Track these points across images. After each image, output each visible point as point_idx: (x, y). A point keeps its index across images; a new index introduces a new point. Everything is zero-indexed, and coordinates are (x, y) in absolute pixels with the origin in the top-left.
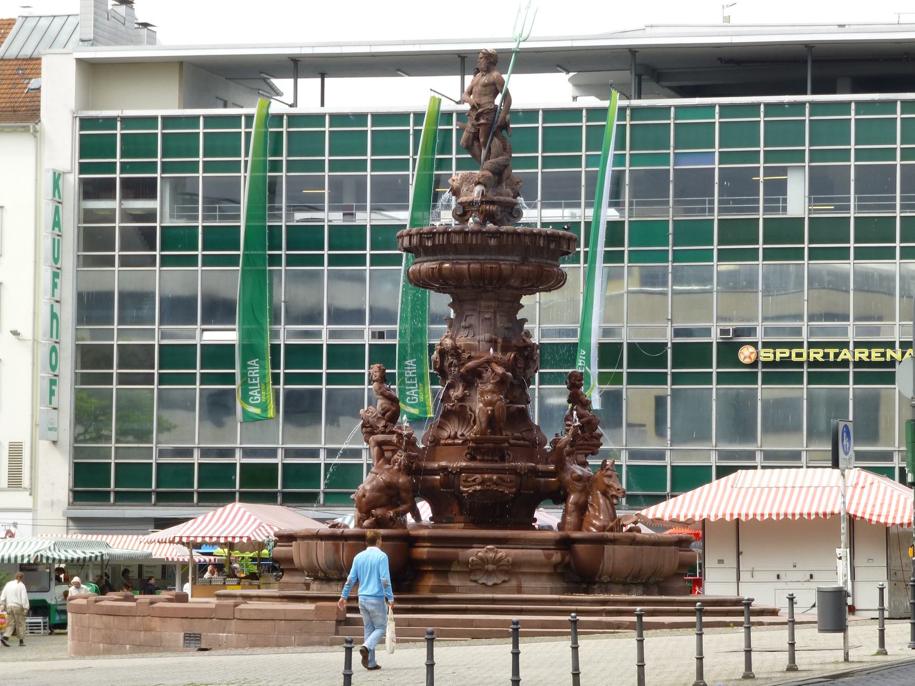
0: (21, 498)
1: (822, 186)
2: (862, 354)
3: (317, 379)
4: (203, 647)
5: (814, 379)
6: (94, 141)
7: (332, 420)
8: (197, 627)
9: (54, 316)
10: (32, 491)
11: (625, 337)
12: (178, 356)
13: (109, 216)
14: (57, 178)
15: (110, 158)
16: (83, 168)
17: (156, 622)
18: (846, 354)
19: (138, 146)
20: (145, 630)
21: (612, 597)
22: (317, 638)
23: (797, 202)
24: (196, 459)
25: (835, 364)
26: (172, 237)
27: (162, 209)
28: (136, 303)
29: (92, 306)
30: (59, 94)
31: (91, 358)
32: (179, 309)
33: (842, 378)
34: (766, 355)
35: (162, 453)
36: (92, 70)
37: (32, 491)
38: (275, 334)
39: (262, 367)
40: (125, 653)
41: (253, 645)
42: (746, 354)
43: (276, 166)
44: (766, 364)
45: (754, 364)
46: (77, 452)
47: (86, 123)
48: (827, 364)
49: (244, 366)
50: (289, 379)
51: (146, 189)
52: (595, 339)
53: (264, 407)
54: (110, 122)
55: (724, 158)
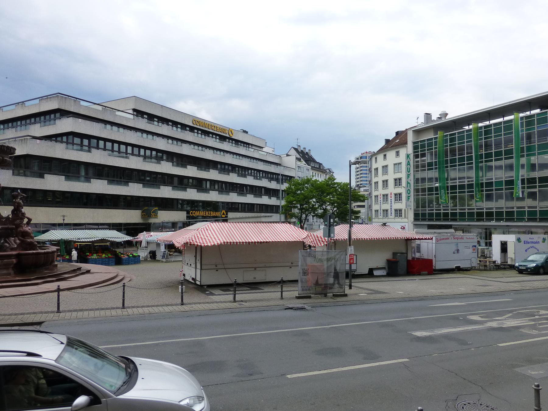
0: (406, 220)
3: (456, 193)
6: (415, 148)
7: (496, 201)
9: (408, 183)
10: (407, 218)
11: (525, 177)
12: (431, 189)
13: (418, 162)
14: (408, 156)
15: (419, 150)
16: (414, 152)
19: (423, 146)
24: (434, 212)
26: (430, 164)
27: (427, 159)
28: (423, 180)
29: (417, 181)
30: (411, 138)
31: (417, 191)
32: (430, 180)
35: (429, 210)
36: (418, 132)
37: (407, 218)
38: (448, 183)
39: (445, 191)
43: (447, 146)
46: (415, 210)
47: (414, 143)
49: (440, 191)
50: (451, 193)
51: (423, 155)
52: (520, 178)
53: (445, 200)
54: (418, 142)
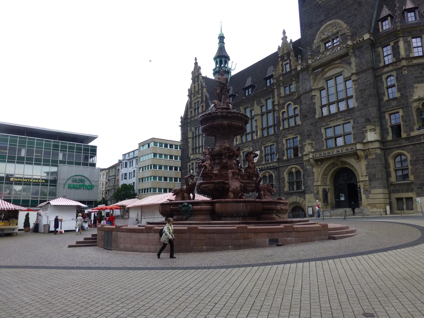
1: (29, 152)
2: (34, 181)
4: (280, 244)
5: (24, 184)
8: (275, 236)
17: (252, 235)
18: (31, 180)
20: (244, 239)
21: (226, 222)
22: (323, 237)
23: (23, 153)
25: (29, 182)
33: (30, 185)
34: (16, 180)
40: (229, 249)
41: (302, 242)
42: (12, 179)
44: (15, 181)
45: (13, 181)
48: (28, 182)
55: (10, 145)
